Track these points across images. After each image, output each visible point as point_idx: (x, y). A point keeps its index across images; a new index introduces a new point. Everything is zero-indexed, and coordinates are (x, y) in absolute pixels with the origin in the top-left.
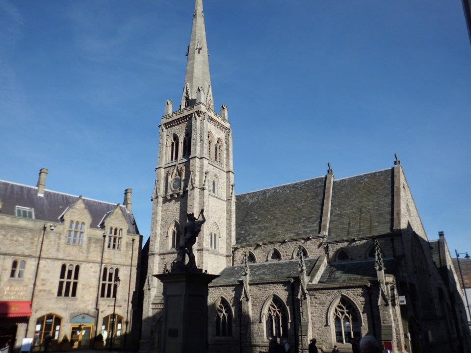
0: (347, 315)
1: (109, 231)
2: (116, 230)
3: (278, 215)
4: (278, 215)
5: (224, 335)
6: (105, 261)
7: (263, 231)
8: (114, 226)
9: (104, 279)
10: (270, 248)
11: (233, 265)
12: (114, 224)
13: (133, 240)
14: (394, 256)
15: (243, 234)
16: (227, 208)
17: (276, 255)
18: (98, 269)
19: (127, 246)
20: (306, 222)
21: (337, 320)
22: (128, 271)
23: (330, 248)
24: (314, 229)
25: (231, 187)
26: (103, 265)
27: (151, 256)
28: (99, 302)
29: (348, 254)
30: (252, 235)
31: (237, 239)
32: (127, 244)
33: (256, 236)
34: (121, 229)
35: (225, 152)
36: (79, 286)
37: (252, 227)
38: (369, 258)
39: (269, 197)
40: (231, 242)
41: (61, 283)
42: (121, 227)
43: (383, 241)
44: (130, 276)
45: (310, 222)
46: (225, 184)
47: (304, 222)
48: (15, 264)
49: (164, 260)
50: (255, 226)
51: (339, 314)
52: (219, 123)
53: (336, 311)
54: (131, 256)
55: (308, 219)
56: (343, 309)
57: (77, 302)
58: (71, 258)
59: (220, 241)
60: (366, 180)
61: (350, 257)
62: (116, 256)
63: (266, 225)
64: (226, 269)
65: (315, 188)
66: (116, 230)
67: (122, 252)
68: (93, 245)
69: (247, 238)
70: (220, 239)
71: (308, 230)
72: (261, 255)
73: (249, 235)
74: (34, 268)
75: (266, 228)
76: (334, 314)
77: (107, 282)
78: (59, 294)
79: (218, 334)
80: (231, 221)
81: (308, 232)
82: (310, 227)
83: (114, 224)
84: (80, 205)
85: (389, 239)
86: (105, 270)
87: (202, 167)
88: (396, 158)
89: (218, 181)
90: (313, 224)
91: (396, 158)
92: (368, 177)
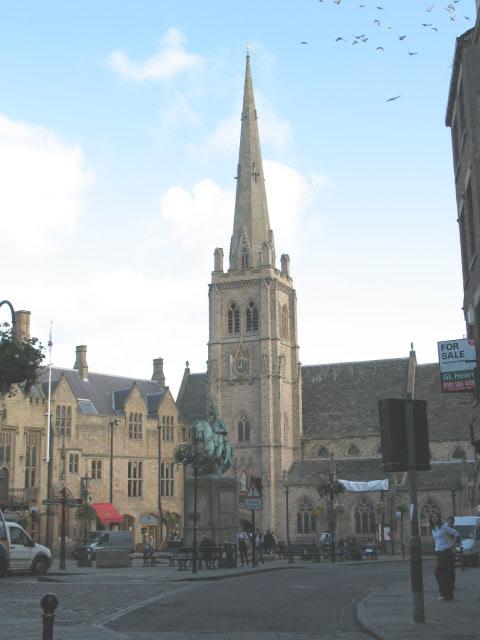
1: (161, 419)
3: (353, 403)
5: (307, 531)
7: (335, 420)
9: (163, 476)
17: (354, 449)
18: (157, 466)
28: (163, 502)
31: (305, 428)
35: (289, 321)
36: (144, 485)
38: (451, 458)
39: (338, 377)
41: (129, 482)
48: (93, 464)
50: (326, 415)
57: (145, 502)
58: (135, 455)
63: (340, 413)
64: (294, 463)
68: (151, 438)
69: (317, 428)
74: (108, 467)
75: (339, 417)
77: (165, 479)
78: (129, 495)
79: (300, 530)
84: (136, 394)
86: (163, 465)
87: (275, 349)
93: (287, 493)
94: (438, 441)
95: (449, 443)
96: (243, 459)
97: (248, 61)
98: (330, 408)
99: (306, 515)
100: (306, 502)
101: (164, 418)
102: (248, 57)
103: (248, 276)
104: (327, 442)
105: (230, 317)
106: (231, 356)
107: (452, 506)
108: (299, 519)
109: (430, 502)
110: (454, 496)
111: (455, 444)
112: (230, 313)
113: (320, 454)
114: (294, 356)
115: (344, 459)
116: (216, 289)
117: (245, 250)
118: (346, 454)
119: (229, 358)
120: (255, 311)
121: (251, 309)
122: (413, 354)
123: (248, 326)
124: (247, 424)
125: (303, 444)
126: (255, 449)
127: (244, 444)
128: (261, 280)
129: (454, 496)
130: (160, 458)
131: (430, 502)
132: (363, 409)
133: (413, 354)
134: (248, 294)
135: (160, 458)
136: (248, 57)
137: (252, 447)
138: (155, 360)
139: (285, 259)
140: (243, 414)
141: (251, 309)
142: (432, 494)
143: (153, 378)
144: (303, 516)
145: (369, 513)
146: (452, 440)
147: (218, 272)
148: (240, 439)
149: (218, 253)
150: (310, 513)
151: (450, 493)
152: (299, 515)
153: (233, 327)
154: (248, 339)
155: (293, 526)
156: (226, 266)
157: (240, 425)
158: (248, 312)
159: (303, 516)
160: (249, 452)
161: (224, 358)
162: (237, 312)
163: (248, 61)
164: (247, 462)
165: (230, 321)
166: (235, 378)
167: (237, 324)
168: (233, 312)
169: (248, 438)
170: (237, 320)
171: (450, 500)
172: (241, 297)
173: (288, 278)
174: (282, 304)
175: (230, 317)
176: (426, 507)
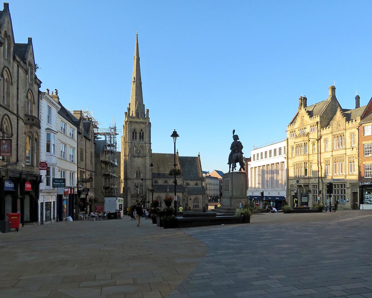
10: (164, 179)
17: (166, 182)
21: (194, 202)
23: (184, 182)
96: (138, 183)
106: (135, 148)
110: (203, 196)
112: (133, 133)
120: (143, 133)
124: (140, 171)
129: (203, 196)
134: (139, 126)
142: (197, 196)
145: (178, 201)
146: (196, 180)
148: (137, 177)
157: (137, 172)
158: (140, 133)
162: (136, 132)
165: (133, 135)
176: (195, 199)
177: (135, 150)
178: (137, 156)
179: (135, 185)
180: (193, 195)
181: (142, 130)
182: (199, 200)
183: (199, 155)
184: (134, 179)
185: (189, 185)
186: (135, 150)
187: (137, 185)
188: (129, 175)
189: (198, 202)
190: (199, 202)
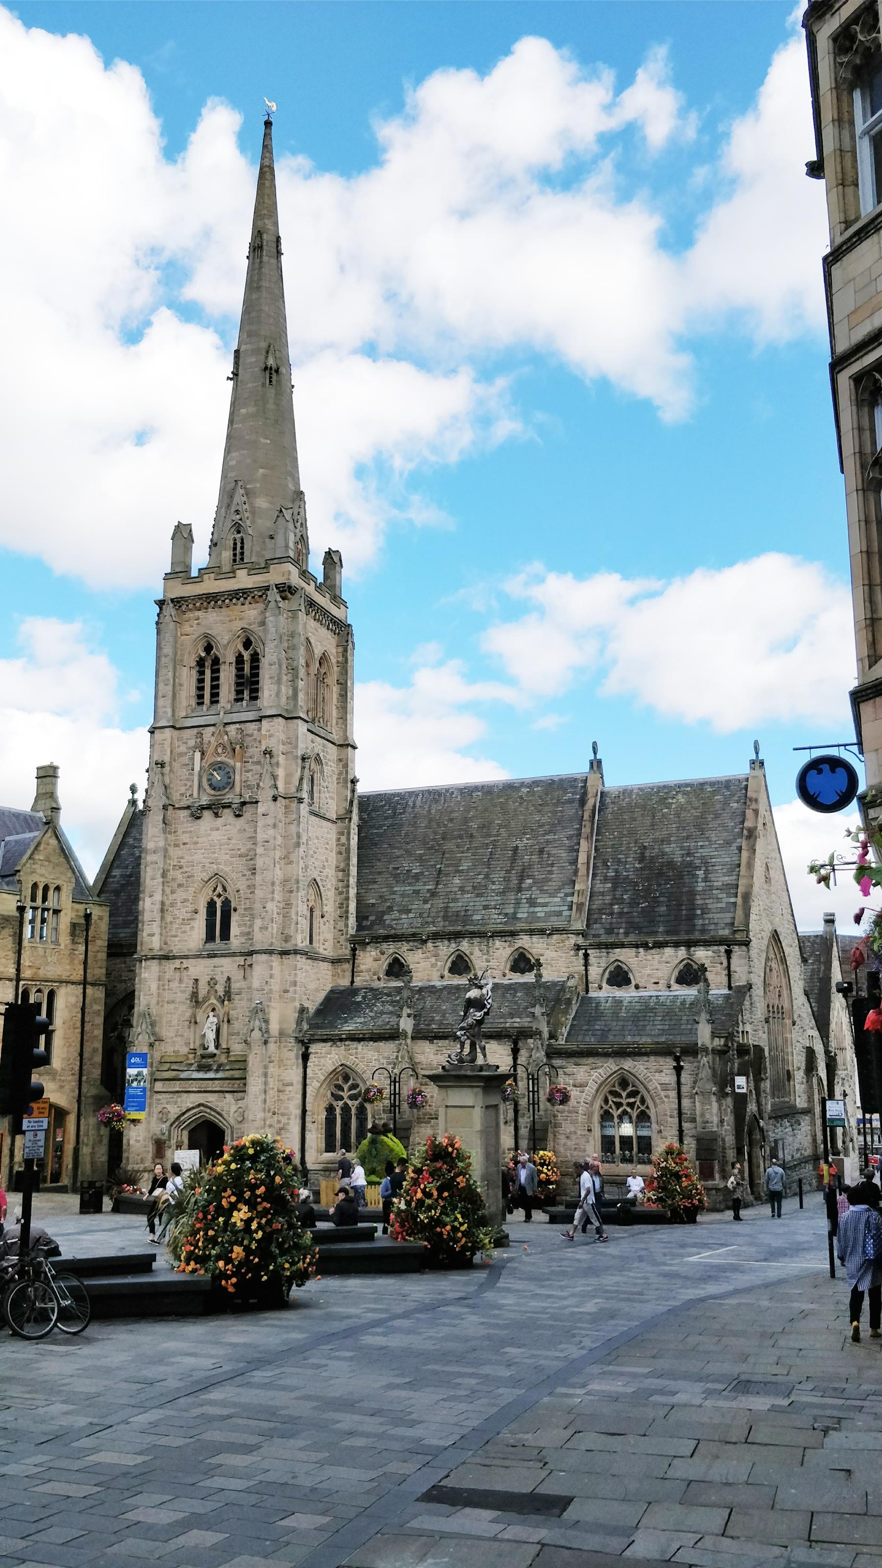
0: (629, 1110)
2: (46, 888)
4: (464, 866)
6: (26, 973)
7: (426, 902)
8: (43, 879)
10: (446, 949)
11: (352, 982)
12: (41, 875)
13: (88, 917)
14: (730, 988)
15: (373, 905)
16: (338, 840)
19: (73, 934)
20: (535, 892)
21: (606, 1116)
22: (77, 996)
23: (592, 960)
24: (553, 909)
25: (349, 785)
26: (22, 983)
27: (148, 963)
29: (631, 976)
30: (399, 911)
32: (74, 926)
33: (411, 915)
34: (58, 889)
35: (335, 689)
37: (395, 889)
38: (675, 986)
40: (347, 926)
42: (59, 882)
43: (710, 953)
44: (83, 1009)
45: (546, 892)
46: (335, 777)
47: (529, 888)
49: (185, 973)
51: (611, 1107)
52: (325, 613)
53: (606, 1101)
54: (82, 957)
55: (540, 884)
56: (620, 1096)
59: (322, 925)
60: (681, 799)
61: (633, 983)
62: (50, 959)
65: (556, 805)
66: (46, 888)
67: (62, 947)
70: (322, 920)
71: (540, 912)
72: (423, 964)
73: (390, 908)
76: (602, 1107)
79: (330, 1147)
80: (348, 875)
81: (539, 915)
82: (545, 905)
83: (41, 875)
85: (722, 948)
88: (757, 753)
89: (322, 772)
90: (552, 895)
91: (757, 753)
92: (685, 793)
93: (305, 1057)
94: (645, 946)
95: (669, 951)
96: (212, 983)
97: (267, 136)
98: (417, 877)
99: (346, 1109)
100: (346, 1078)
101: (35, 886)
102: (268, 124)
103: (244, 580)
104: (405, 946)
105: (201, 673)
106: (198, 755)
107: (673, 1094)
108: (330, 1122)
109: (624, 1083)
111: (682, 952)
112: (201, 663)
113: (389, 973)
114: (345, 764)
115: (438, 984)
116: (169, 609)
117: (238, 528)
118: (446, 973)
119: (192, 759)
120: (255, 658)
121: (246, 655)
122: (596, 765)
123: (239, 692)
124: (226, 903)
125: (354, 950)
126: (240, 960)
127: (218, 944)
128: (267, 588)
129: (678, 1070)
130: (18, 979)
131: (624, 1083)
132: (487, 876)
133: (596, 765)
135: (18, 979)
136: (268, 124)
137: (234, 955)
138: (55, 768)
139: (332, 559)
140: (217, 879)
141: (246, 655)
142: (628, 1064)
143: (34, 809)
144: (338, 1111)
146: (676, 945)
147: (179, 571)
148: (210, 937)
149: (183, 535)
150: (353, 1105)
151: (670, 1063)
152: (330, 1110)
153: (207, 693)
154: (235, 717)
155: (315, 1137)
156: (200, 556)
157: (211, 905)
158: (240, 660)
159: (338, 1111)
160: (228, 967)
161: (185, 759)
162: (216, 661)
163: (267, 136)
164: (220, 989)
165: (201, 681)
166: (205, 800)
167: (215, 687)
168: (208, 661)
169: (226, 935)
170: (215, 679)
171: (670, 1078)
172: (224, 627)
173: (337, 599)
174: (318, 652)
175: (201, 673)
177: (197, 767)
178: (208, 807)
179: (194, 995)
180: (599, 1061)
181: (247, 644)
182: (649, 1101)
183: (758, 764)
184: (186, 957)
185: (628, 982)
186: (197, 767)
187: (203, 990)
188: (155, 928)
189: (643, 1118)
190: (652, 1113)
